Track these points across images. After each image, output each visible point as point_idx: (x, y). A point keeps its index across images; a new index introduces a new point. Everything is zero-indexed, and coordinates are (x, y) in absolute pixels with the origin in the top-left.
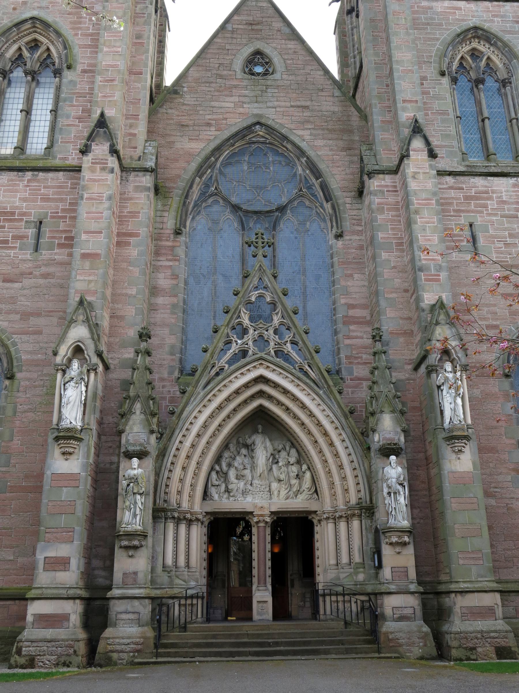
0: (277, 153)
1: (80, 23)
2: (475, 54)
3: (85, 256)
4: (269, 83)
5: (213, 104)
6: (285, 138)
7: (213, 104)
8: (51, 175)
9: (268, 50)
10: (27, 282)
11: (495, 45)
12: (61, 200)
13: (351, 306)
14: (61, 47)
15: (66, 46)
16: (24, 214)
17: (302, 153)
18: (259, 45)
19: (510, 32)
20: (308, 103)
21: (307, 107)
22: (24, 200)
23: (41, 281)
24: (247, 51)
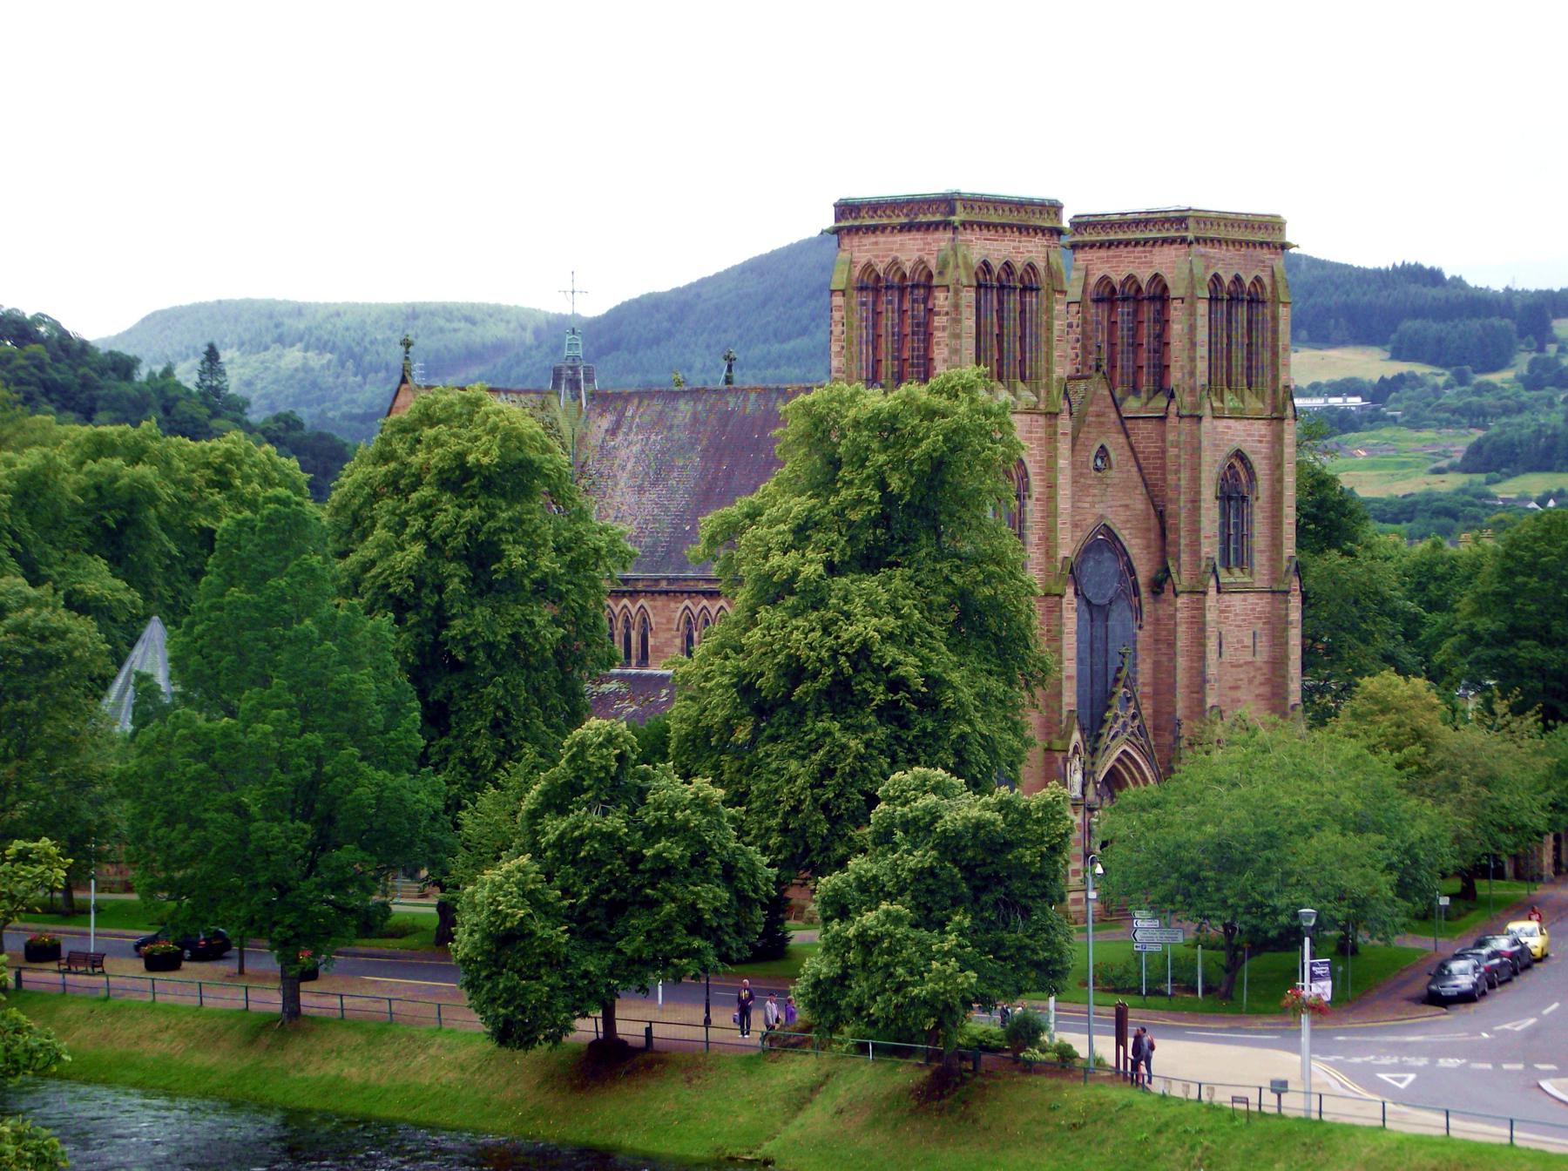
0: (1110, 550)
4: (1109, 481)
9: (1108, 447)
11: (1245, 465)
14: (1021, 472)
15: (1026, 475)
18: (1103, 441)
24: (1097, 446)
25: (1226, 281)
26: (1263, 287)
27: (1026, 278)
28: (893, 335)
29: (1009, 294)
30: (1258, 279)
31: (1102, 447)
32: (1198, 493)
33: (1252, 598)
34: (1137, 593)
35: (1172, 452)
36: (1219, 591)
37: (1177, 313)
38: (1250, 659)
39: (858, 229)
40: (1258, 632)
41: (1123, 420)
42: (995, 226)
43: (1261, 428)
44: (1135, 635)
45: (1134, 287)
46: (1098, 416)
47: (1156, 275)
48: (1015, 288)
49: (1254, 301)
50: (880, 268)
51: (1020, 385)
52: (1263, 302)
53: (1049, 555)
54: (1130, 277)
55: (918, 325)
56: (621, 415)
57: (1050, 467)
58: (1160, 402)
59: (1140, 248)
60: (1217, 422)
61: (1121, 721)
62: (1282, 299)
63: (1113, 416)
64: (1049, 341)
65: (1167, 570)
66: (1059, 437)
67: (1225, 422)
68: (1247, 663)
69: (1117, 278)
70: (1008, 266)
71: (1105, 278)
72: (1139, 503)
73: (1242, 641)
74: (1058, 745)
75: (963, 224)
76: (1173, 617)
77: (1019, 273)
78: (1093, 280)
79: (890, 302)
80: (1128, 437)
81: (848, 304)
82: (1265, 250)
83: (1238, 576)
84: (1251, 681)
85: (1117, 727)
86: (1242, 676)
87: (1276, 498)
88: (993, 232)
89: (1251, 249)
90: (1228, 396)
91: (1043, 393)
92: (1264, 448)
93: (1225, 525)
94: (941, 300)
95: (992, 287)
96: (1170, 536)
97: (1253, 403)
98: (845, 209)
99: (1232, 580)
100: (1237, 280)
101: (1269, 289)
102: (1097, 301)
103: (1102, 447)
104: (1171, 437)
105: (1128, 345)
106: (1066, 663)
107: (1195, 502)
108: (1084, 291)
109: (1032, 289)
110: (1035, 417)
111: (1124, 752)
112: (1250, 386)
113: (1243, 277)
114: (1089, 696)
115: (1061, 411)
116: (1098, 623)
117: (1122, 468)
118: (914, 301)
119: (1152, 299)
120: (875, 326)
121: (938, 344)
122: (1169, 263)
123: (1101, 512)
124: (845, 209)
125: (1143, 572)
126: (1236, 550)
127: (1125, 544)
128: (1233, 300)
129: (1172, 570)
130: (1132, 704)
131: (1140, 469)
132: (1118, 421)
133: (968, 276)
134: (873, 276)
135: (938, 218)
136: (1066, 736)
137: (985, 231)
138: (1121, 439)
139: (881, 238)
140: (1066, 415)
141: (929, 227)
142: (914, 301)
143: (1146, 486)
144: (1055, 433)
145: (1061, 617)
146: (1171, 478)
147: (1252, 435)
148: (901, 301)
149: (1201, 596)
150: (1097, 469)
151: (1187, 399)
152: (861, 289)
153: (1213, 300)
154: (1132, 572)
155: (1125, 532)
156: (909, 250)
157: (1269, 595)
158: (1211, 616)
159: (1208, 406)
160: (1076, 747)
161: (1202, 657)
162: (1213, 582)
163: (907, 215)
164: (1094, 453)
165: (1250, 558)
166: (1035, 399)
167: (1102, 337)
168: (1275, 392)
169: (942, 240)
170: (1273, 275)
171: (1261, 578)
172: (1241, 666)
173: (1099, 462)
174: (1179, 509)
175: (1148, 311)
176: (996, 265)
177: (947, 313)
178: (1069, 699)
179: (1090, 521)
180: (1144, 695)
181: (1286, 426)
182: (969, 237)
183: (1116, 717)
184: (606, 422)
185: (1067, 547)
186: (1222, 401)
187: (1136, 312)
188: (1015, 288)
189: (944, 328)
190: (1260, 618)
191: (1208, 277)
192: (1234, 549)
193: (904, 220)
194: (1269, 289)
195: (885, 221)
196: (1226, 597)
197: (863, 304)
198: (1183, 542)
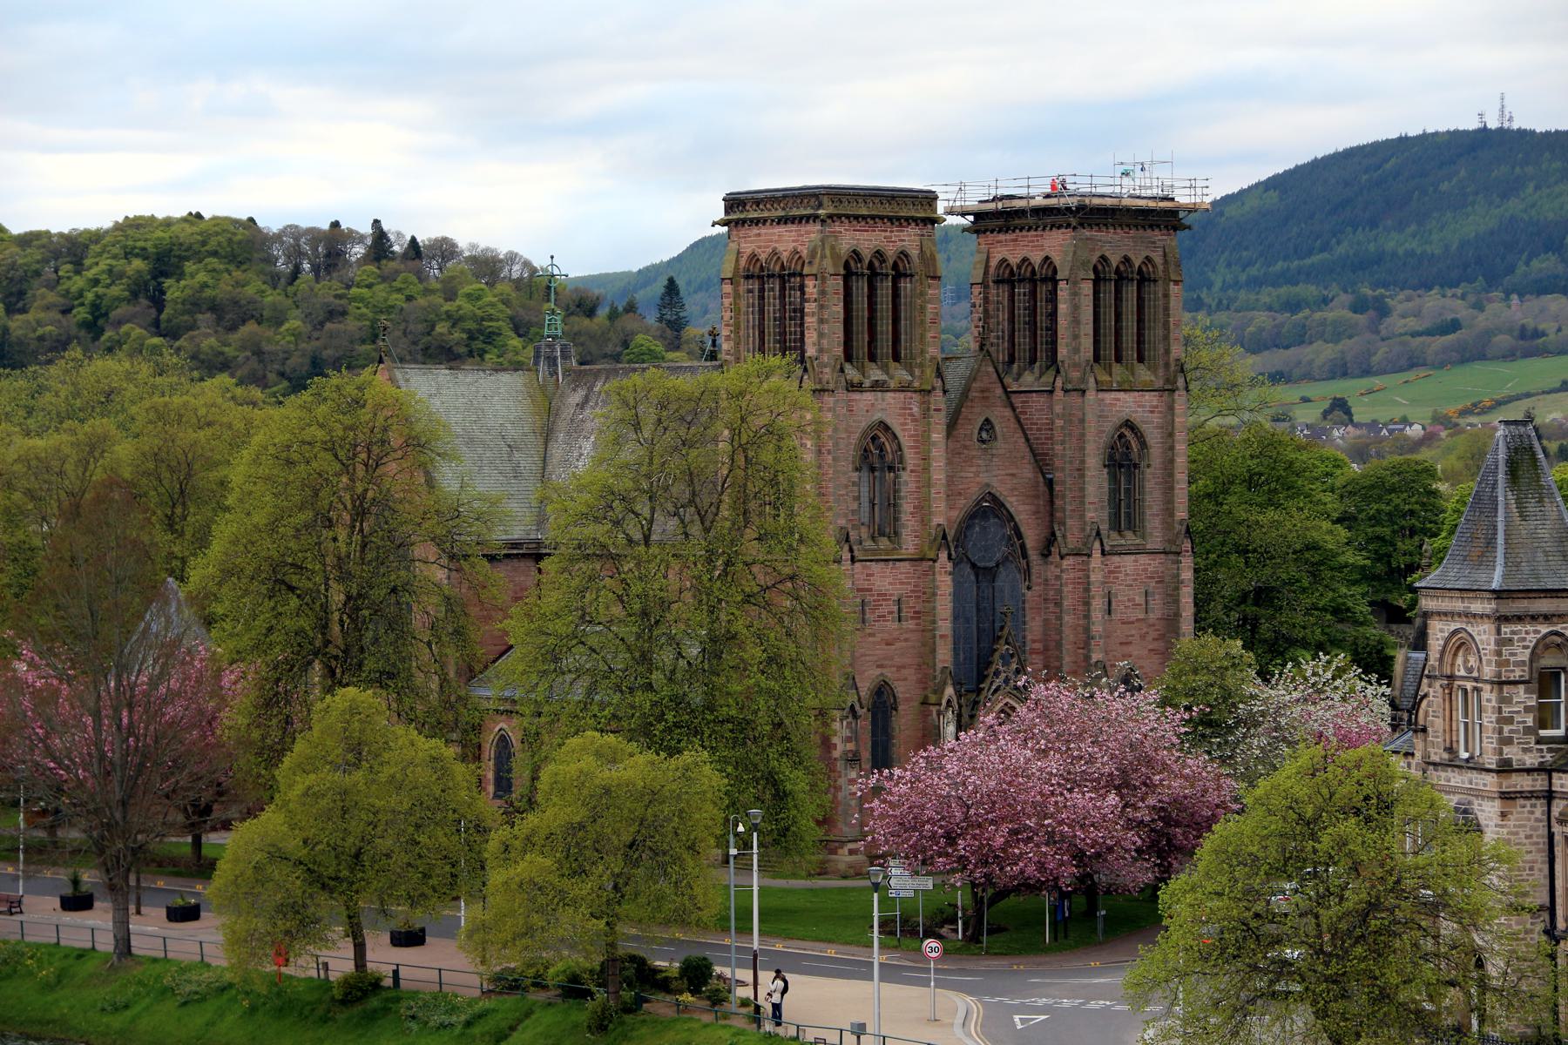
0: (997, 516)
1: (906, 424)
2: (1121, 436)
3: (941, 636)
4: (994, 452)
5: (963, 474)
6: (1003, 505)
7: (963, 474)
8: (902, 564)
9: (992, 419)
10: (898, 645)
12: (909, 583)
13: (1034, 641)
14: (895, 447)
15: (900, 450)
16: (891, 595)
17: (1011, 518)
19: (1146, 422)
20: (1014, 471)
21: (1013, 475)
22: (890, 584)
23: (904, 644)
25: (1115, 261)
26: (1154, 266)
27: (901, 265)
28: (775, 320)
29: (882, 281)
30: (1147, 257)
31: (987, 420)
32: (1083, 462)
33: (1143, 559)
34: (1025, 555)
35: (1059, 423)
36: (1103, 553)
37: (1063, 291)
38: (1142, 616)
39: (744, 221)
40: (1151, 590)
41: (1008, 393)
42: (864, 218)
43: (1150, 399)
44: (1024, 595)
45: (1030, 269)
46: (982, 391)
47: (1047, 258)
48: (887, 275)
49: (1144, 279)
50: (763, 257)
51: (892, 365)
52: (1155, 281)
53: (924, 522)
54: (1025, 260)
55: (795, 311)
56: (590, 389)
57: (923, 441)
58: (1048, 377)
59: (1033, 233)
60: (1101, 395)
61: (1003, 676)
62: (1173, 278)
63: (999, 391)
64: (922, 322)
65: (1053, 534)
66: (932, 412)
67: (1113, 395)
68: (1138, 620)
69: (1014, 260)
70: (879, 254)
71: (1004, 260)
72: (1027, 472)
73: (1134, 600)
74: (933, 698)
75: (831, 216)
76: (1058, 578)
77: (891, 262)
78: (994, 263)
79: (772, 289)
80: (1014, 409)
81: (736, 292)
82: (1157, 232)
83: (1130, 539)
84: (1143, 637)
85: (998, 681)
86: (1133, 632)
87: (1169, 463)
88: (863, 223)
89: (1141, 231)
90: (1117, 368)
91: (917, 372)
92: (1156, 419)
93: (1114, 492)
94: (811, 287)
95: (863, 275)
96: (1058, 502)
97: (1144, 374)
98: (734, 203)
99: (1123, 542)
100: (1127, 260)
101: (1161, 268)
102: (997, 282)
103: (987, 420)
104: (1058, 409)
105: (1025, 323)
106: (940, 623)
107: (1081, 471)
108: (986, 273)
109: (906, 275)
110: (909, 394)
111: (1006, 704)
112: (1141, 359)
113: (1133, 258)
114: (975, 652)
115: (934, 388)
116: (984, 585)
117: (1008, 438)
118: (790, 289)
119: (1044, 280)
120: (762, 312)
121: (809, 329)
122: (1055, 245)
123: (986, 481)
124: (734, 203)
125: (1032, 536)
126: (1128, 515)
127: (1012, 510)
128: (1121, 278)
129: (1058, 534)
130: (1015, 659)
131: (1027, 440)
132: (1004, 397)
133: (835, 265)
134: (758, 265)
135: (809, 211)
136: (939, 691)
137: (855, 223)
138: (1008, 413)
139: (763, 230)
140: (939, 393)
141: (800, 220)
142: (790, 289)
143: (1035, 455)
144: (928, 409)
145: (934, 580)
146: (1058, 447)
147: (1143, 406)
148: (783, 289)
149: (1085, 558)
150: (983, 442)
151: (1075, 375)
152: (747, 277)
153: (1097, 282)
154: (1019, 536)
155: (1013, 499)
156: (785, 241)
157: (1162, 556)
158: (1095, 577)
159: (1092, 380)
160: (949, 701)
161: (1087, 617)
162: (1097, 545)
163: (784, 209)
164: (978, 427)
165: (1142, 521)
166: (910, 378)
167: (1003, 316)
168: (1167, 365)
169: (813, 232)
170: (1165, 255)
171: (1155, 540)
172: (1133, 623)
173: (984, 435)
174: (1063, 476)
175: (1042, 290)
176: (867, 255)
177: (815, 300)
178: (944, 655)
179: (974, 492)
180: (1033, 651)
181: (1176, 397)
182: (837, 229)
183: (997, 674)
184: (577, 397)
185: (943, 515)
186: (1111, 375)
187: (1033, 294)
188: (887, 275)
189: (813, 314)
190: (1153, 578)
191: (1094, 259)
192: (1124, 513)
193: (780, 213)
194: (1161, 268)
195: (766, 214)
196: (1116, 559)
197: (750, 291)
198: (1068, 507)
